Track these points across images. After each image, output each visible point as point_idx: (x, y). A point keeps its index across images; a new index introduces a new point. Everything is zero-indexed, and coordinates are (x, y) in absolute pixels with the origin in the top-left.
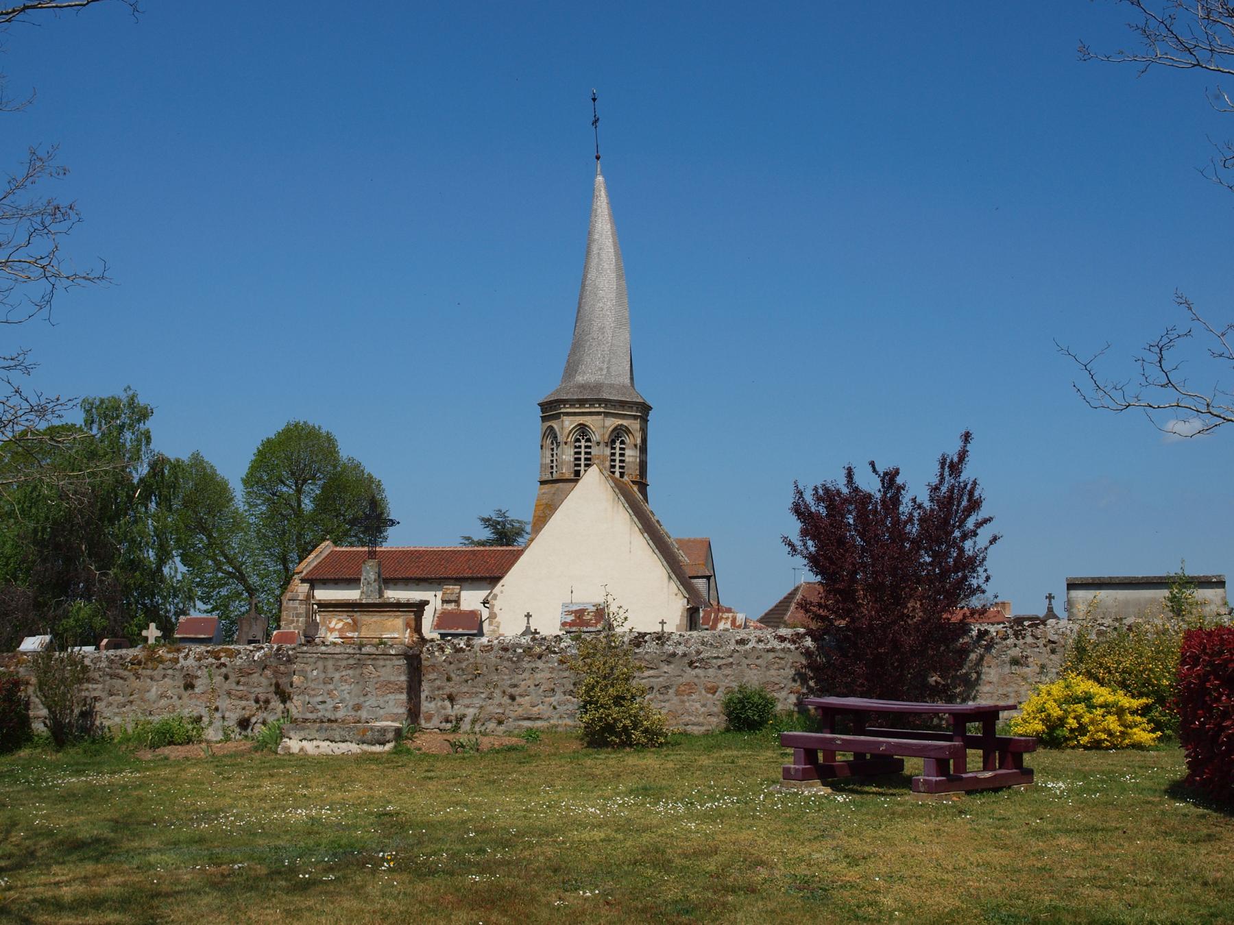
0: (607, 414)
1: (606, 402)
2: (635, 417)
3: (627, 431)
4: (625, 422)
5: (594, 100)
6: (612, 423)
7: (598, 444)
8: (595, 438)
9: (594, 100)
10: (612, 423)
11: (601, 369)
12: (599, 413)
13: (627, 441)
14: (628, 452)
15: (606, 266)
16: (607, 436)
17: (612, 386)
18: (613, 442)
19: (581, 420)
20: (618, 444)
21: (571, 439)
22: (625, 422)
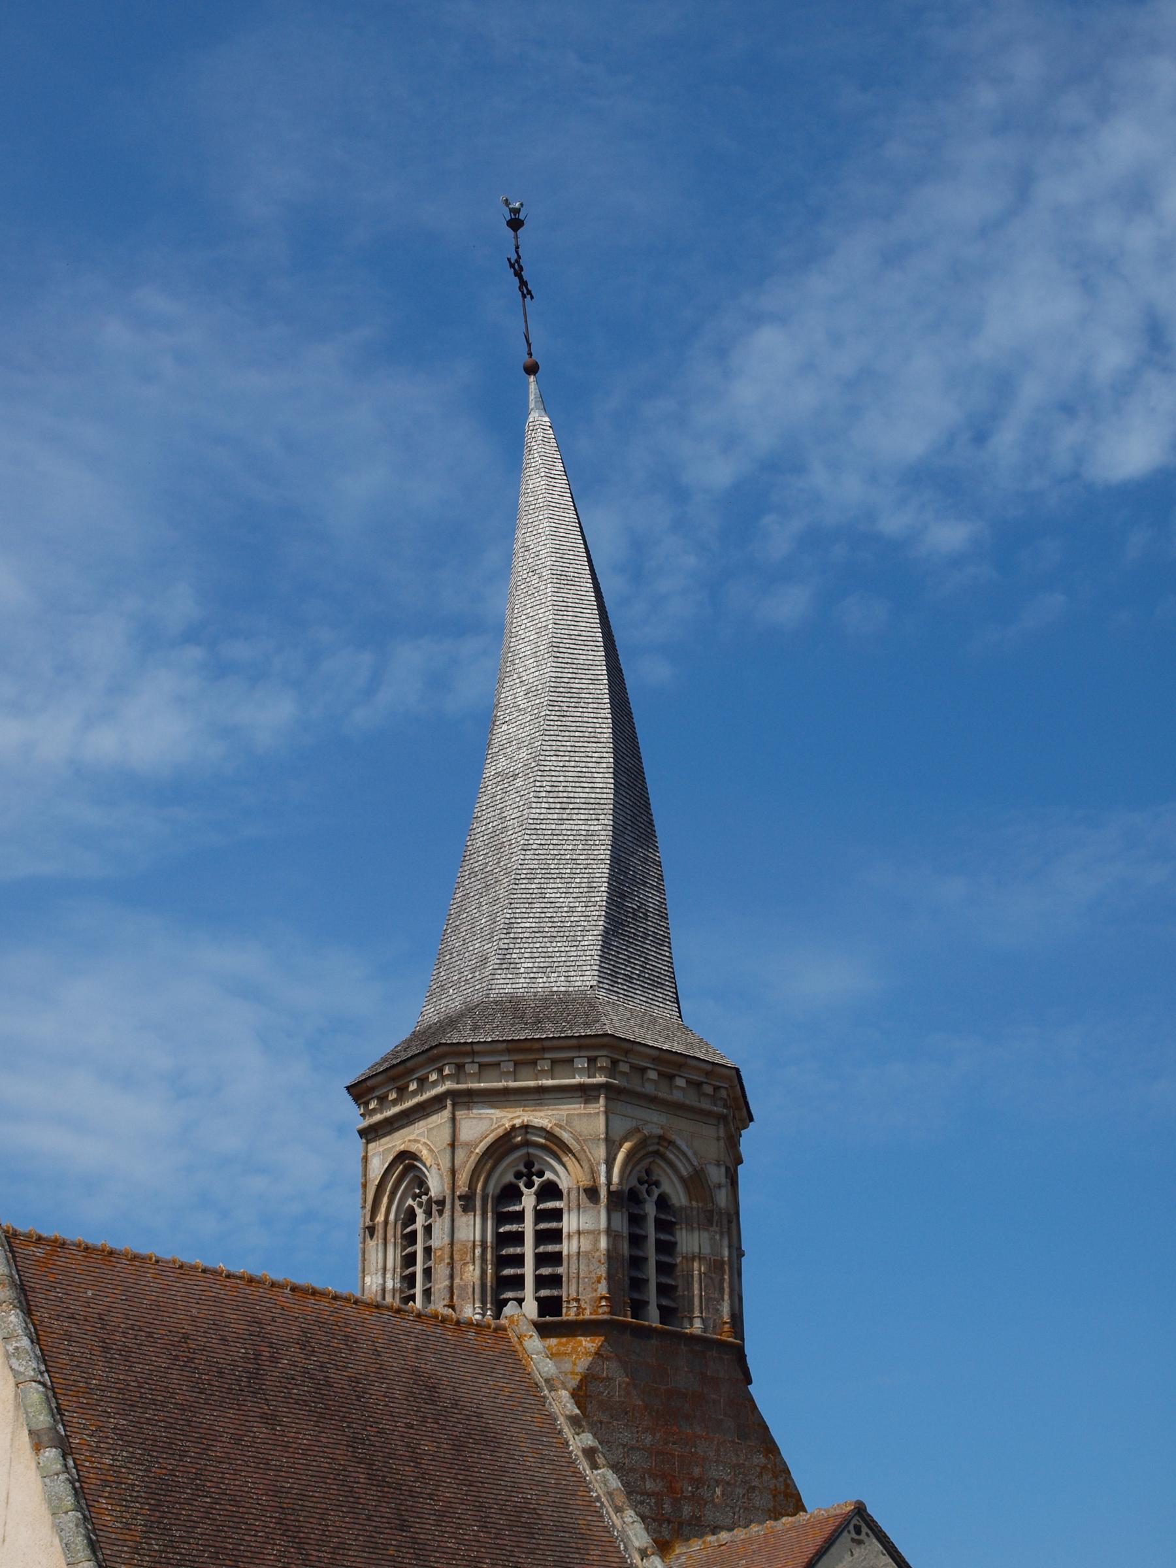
0: (464, 1099)
1: (460, 1056)
2: (585, 1093)
3: (556, 1145)
4: (542, 1117)
5: (515, 224)
6: (483, 1125)
7: (441, 1203)
8: (436, 1185)
9: (515, 224)
10: (483, 1125)
11: (485, 960)
12: (436, 1104)
13: (564, 1185)
14: (569, 1223)
15: (525, 649)
16: (463, 1178)
17: (515, 1007)
18: (512, 1193)
19: (398, 1141)
20: (528, 1201)
21: (388, 1213)
22: (542, 1117)
